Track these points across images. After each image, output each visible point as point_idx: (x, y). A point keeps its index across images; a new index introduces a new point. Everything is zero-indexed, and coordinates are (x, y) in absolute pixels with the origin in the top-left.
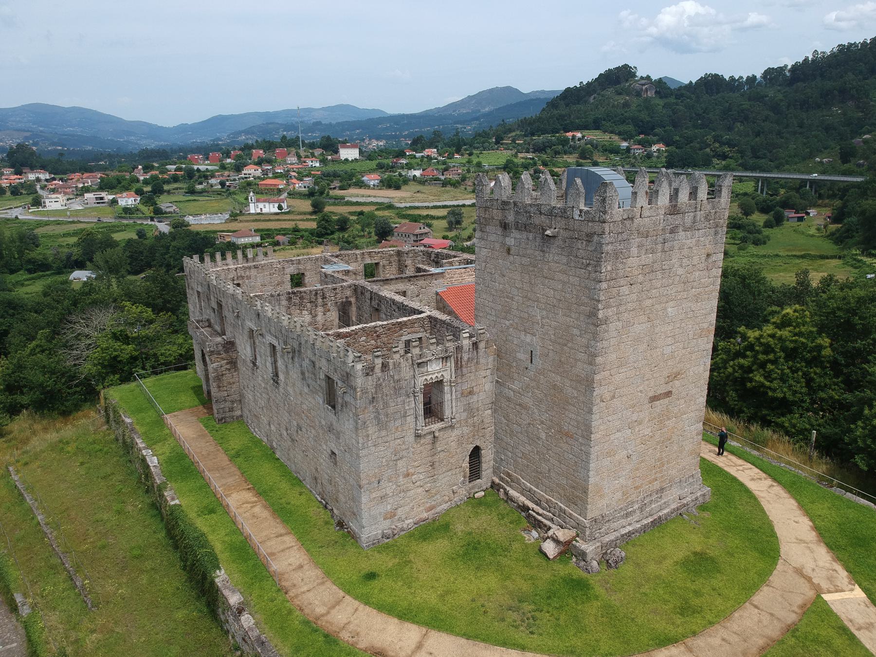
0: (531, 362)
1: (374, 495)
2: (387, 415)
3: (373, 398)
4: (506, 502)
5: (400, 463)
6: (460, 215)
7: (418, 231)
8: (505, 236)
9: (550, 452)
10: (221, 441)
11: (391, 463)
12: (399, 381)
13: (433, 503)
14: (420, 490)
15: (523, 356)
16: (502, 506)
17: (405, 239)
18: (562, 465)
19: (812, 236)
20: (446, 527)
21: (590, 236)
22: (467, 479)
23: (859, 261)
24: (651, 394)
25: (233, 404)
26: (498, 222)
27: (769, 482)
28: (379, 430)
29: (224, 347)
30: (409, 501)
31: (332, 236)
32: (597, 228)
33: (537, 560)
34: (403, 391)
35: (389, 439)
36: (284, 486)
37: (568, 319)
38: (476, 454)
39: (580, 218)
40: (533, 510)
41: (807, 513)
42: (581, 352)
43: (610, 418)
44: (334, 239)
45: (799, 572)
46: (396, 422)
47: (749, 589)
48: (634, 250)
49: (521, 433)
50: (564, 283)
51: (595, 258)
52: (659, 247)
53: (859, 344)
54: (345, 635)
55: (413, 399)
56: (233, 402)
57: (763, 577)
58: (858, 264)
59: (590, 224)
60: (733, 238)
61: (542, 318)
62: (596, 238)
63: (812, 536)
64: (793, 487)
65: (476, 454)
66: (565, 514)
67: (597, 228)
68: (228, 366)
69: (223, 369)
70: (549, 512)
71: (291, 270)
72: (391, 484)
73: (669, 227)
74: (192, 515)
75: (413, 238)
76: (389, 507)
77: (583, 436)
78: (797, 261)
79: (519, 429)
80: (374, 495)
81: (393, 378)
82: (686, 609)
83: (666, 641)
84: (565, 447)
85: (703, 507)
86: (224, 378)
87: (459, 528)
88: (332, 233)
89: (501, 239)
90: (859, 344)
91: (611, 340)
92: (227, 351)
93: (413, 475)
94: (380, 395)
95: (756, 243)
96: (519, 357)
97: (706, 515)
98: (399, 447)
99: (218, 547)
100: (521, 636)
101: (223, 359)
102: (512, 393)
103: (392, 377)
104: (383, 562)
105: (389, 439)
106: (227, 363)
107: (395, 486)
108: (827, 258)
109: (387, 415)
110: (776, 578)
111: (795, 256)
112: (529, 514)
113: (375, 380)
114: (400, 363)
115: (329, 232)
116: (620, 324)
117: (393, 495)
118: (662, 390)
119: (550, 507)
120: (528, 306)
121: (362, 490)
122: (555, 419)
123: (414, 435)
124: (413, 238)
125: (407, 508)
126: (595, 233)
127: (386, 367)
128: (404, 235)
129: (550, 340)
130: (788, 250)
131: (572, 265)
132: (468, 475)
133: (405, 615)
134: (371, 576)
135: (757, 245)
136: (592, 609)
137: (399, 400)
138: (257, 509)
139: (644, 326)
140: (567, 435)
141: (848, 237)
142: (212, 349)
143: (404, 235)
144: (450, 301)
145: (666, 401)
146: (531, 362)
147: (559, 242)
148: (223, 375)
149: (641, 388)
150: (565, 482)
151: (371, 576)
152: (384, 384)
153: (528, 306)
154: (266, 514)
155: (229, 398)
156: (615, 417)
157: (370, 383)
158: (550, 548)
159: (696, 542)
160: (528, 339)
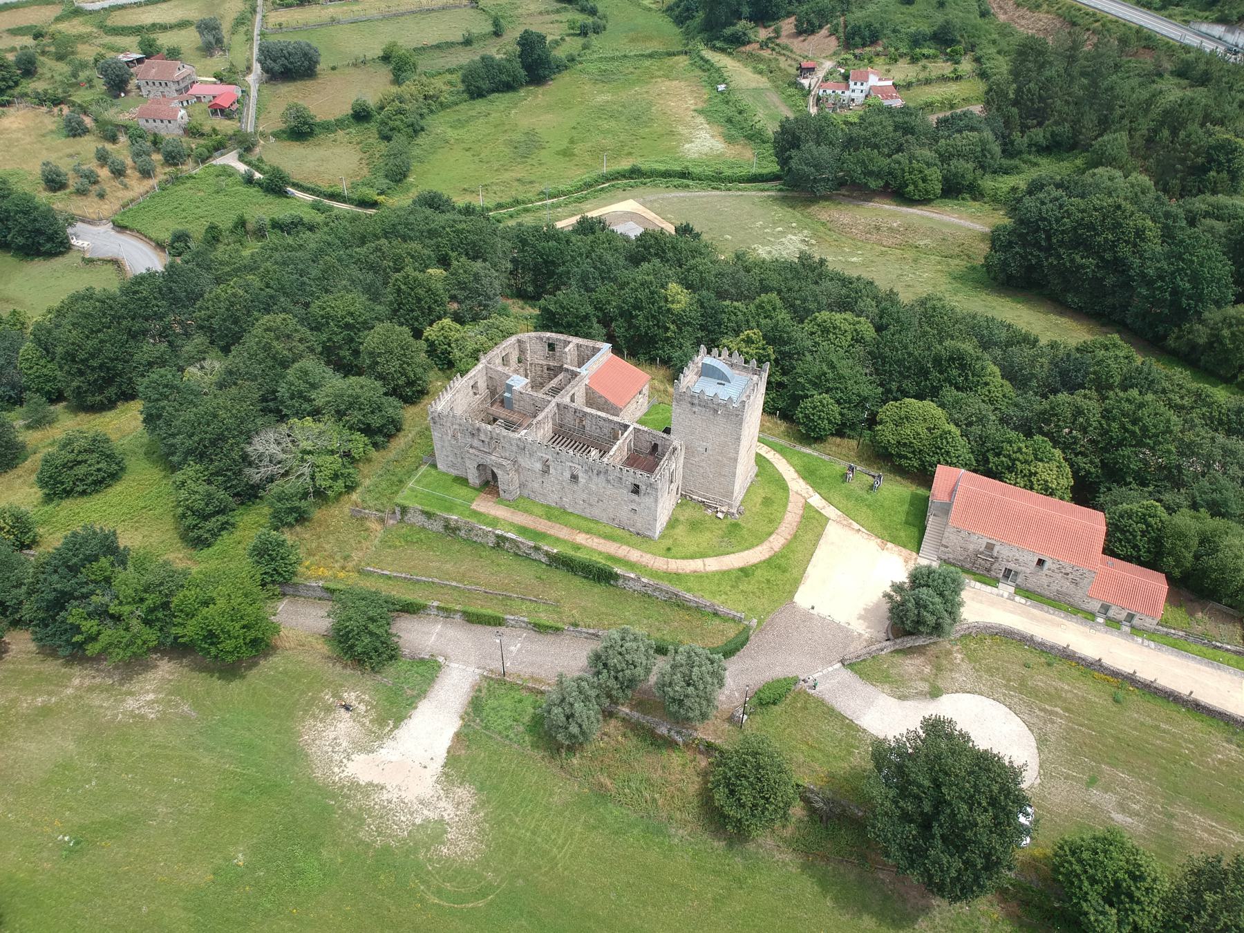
6: (218, 28)
7: (177, 75)
10: (526, 511)
15: (701, 450)
16: (691, 503)
17: (161, 89)
19: (650, 9)
20: (677, 520)
21: (737, 415)
23: (707, 61)
27: (773, 452)
31: (17, 91)
33: (718, 521)
36: (592, 525)
41: (792, 465)
44: (26, 95)
45: (797, 493)
47: (785, 506)
53: (787, 348)
54: (680, 571)
57: (787, 498)
58: (707, 66)
60: (573, 29)
63: (795, 475)
64: (781, 451)
71: (472, 383)
74: (573, 553)
75: (174, 87)
78: (647, 63)
82: (771, 521)
83: (770, 534)
85: (757, 476)
87: (682, 518)
88: (17, 84)
90: (787, 348)
95: (597, 30)
97: (759, 478)
99: (604, 562)
100: (730, 549)
104: (669, 542)
108: (674, 54)
110: (791, 499)
111: (642, 55)
115: (11, 83)
124: (174, 87)
128: (157, 83)
130: (632, 40)
133: (692, 557)
134: (669, 549)
135: (598, 33)
136: (745, 532)
138: (595, 540)
141: (688, 18)
143: (157, 83)
144: (600, 390)
151: (669, 549)
154: (602, 541)
158: (720, 515)
159: (761, 493)
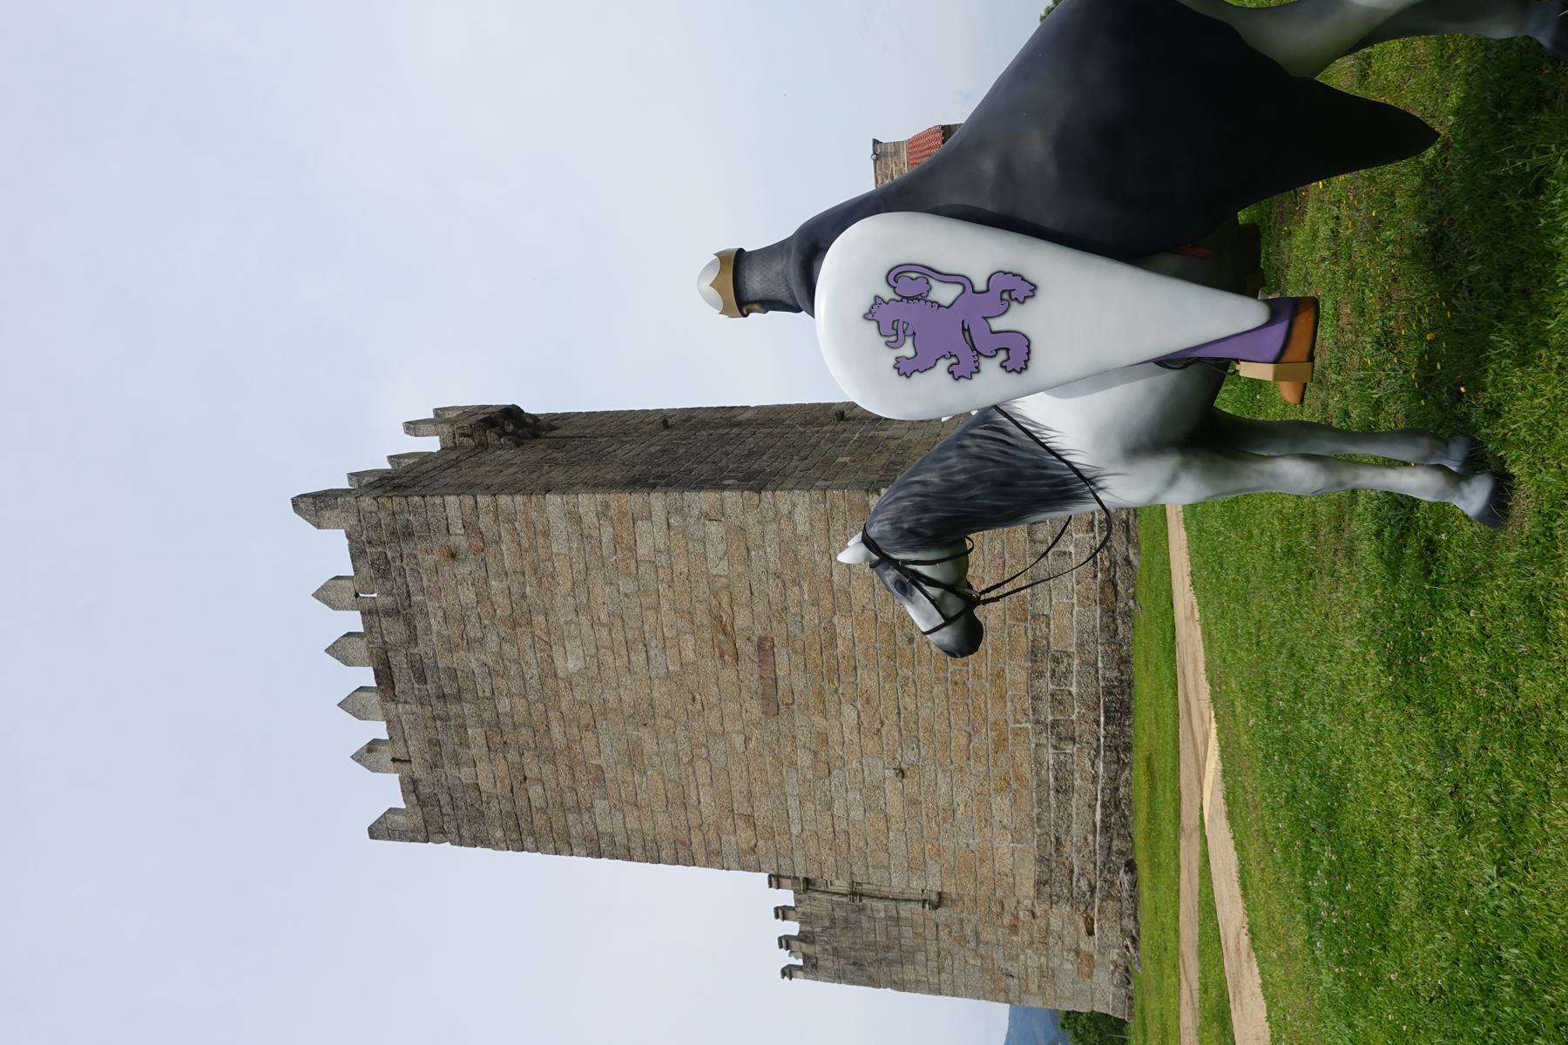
1: (1033, 988)
2: (888, 948)
3: (854, 964)
5: (984, 936)
11: (982, 951)
12: (833, 920)
24: (755, 709)
28: (913, 963)
30: (1071, 929)
34: (852, 916)
35: (932, 948)
43: (795, 830)
46: (906, 934)
48: (466, 774)
52: (453, 709)
72: (1022, 957)
73: (416, 686)
76: (1068, 966)
80: (1033, 988)
81: (827, 928)
91: (629, 826)
93: (1017, 918)
94: (853, 953)
98: (954, 934)
103: (825, 929)
105: (932, 948)
107: (1029, 952)
109: (888, 948)
113: (826, 957)
114: (804, 914)
116: (601, 805)
117: (1047, 956)
118: (750, 672)
127: (807, 937)
137: (865, 924)
139: (605, 739)
145: (782, 657)
149: (738, 741)
152: (835, 944)
156: (794, 814)
157: (829, 964)
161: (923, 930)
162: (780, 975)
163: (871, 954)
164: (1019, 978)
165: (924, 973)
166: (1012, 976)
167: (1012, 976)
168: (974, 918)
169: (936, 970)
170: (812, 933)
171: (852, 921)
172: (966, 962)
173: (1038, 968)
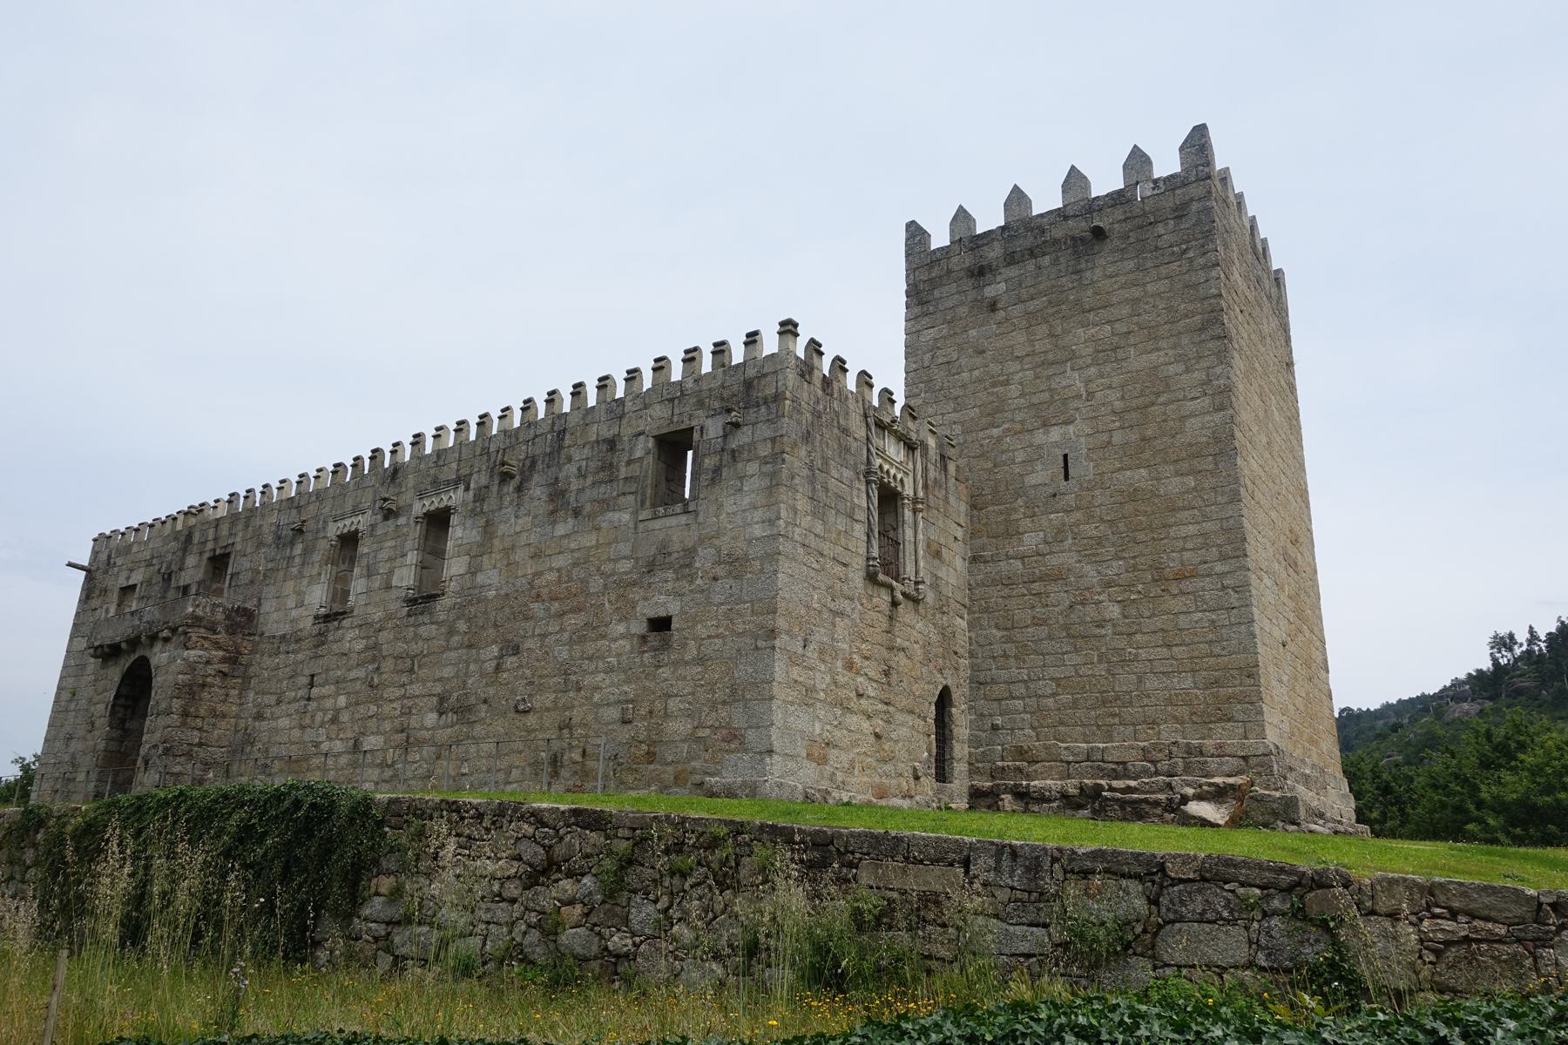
0: (1066, 478)
3: (808, 432)
4: (1026, 811)
8: (979, 288)
9: (1138, 637)
13: (884, 780)
14: (866, 725)
15: (1042, 475)
18: (1175, 649)
22: (933, 760)
25: (206, 771)
26: (962, 274)
29: (228, 617)
32: (1196, 190)
37: (1153, 356)
38: (944, 701)
39: (1155, 192)
40: (1111, 789)
42: (1193, 399)
49: (1050, 637)
50: (1135, 301)
51: (1200, 236)
55: (863, 488)
56: (207, 766)
59: (1178, 192)
61: (1088, 382)
62: (1195, 207)
65: (944, 701)
66: (1202, 754)
67: (1196, 190)
68: (225, 668)
69: (210, 670)
70: (1157, 773)
77: (1223, 558)
79: (1043, 631)
84: (1176, 604)
86: (205, 695)
89: (971, 295)
92: (232, 630)
96: (1033, 482)
98: (839, 584)
101: (219, 647)
102: (1019, 563)
105: (826, 548)
106: (224, 660)
107: (828, 679)
112: (1106, 799)
119: (1154, 762)
120: (1049, 378)
121: (777, 643)
122: (1142, 560)
123: (862, 574)
125: (845, 758)
126: (1192, 200)
129: (1114, 412)
131: (1149, 264)
132: (934, 751)
140: (1180, 577)
142: (199, 612)
146: (1066, 478)
147: (1114, 242)
148: (204, 685)
150: (1189, 683)
153: (1049, 378)
155: (202, 753)
160: (1055, 434)
161: (843, 544)
162: (796, 319)
163: (819, 462)
164: (804, 655)
165: (803, 524)
166: (805, 646)
167: (805, 646)
168: (856, 616)
169: (807, 542)
170: (832, 395)
171: (848, 456)
172: (814, 588)
173: (814, 686)
